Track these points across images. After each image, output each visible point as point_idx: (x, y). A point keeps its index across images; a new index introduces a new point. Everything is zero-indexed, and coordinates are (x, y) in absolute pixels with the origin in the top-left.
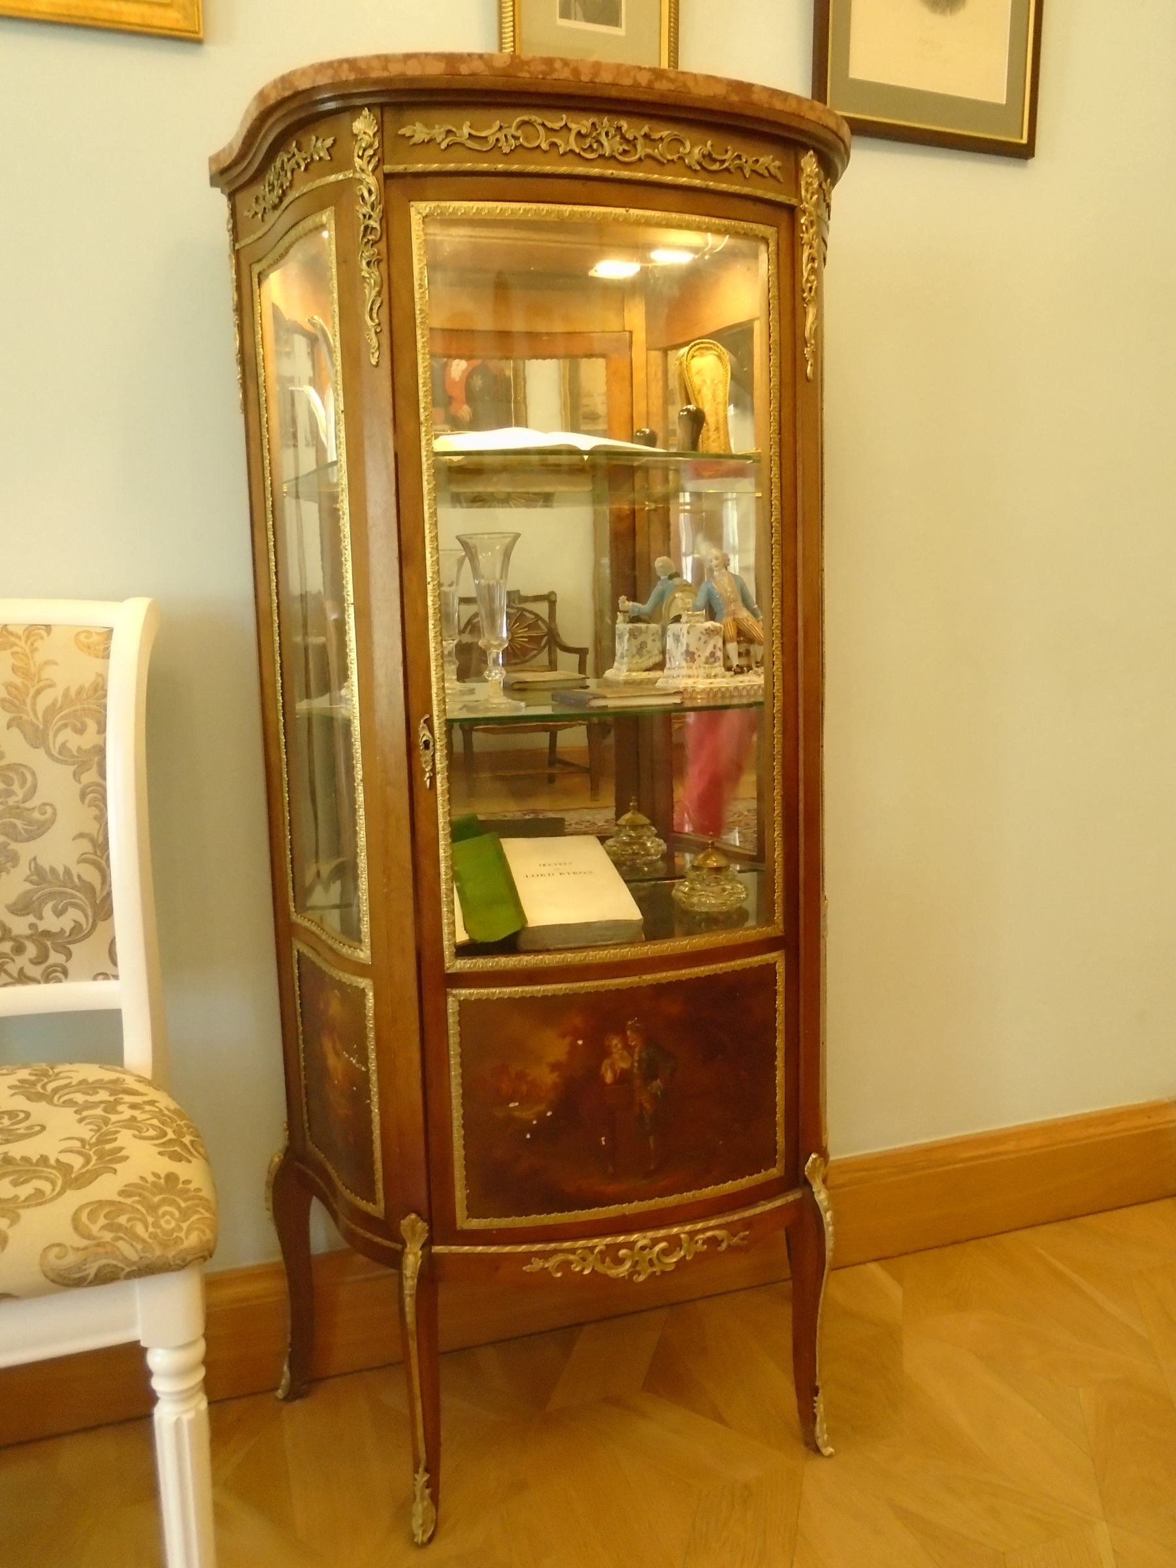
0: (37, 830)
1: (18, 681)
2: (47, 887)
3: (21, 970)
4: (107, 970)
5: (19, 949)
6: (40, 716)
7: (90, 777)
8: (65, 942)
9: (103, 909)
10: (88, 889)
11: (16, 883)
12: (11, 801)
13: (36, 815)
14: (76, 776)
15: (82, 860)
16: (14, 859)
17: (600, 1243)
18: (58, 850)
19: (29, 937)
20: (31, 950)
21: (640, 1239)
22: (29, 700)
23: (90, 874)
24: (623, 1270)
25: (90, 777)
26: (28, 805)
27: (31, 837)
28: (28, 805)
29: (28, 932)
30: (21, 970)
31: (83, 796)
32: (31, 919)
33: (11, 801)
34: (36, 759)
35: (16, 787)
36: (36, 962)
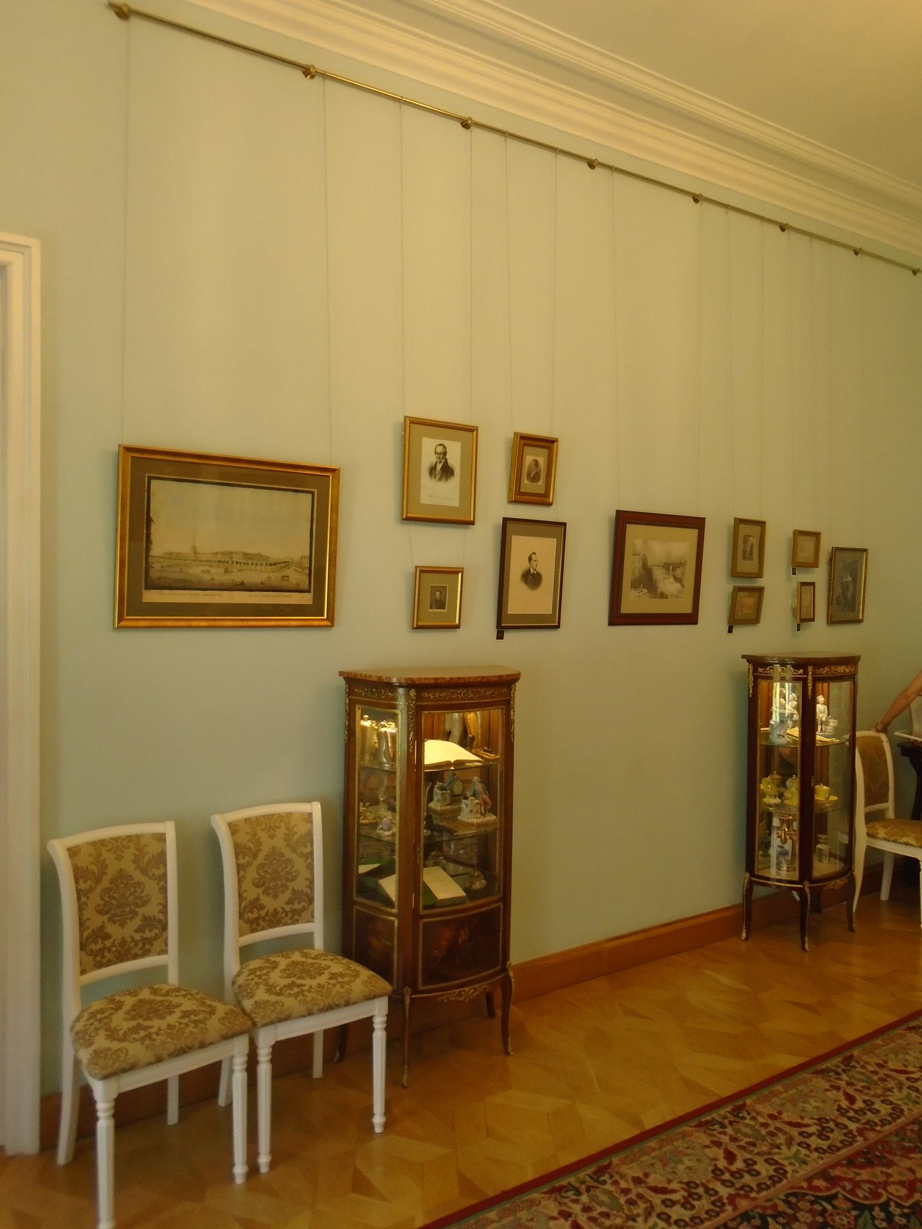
1: (137, 853)
2: (148, 922)
4: (164, 952)
14: (158, 884)
15: (159, 912)
17: (457, 991)
21: (467, 989)
24: (462, 999)
25: (162, 883)
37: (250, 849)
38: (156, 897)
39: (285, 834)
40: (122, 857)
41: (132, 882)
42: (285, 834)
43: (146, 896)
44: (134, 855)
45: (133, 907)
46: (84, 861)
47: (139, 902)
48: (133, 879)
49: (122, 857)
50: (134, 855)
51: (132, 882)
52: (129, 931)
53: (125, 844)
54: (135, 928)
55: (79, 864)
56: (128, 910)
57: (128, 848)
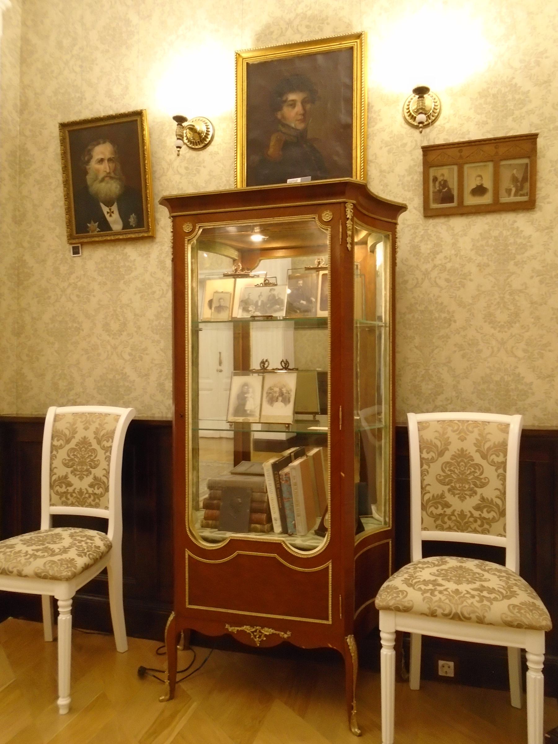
0: (483, 485)
3: (475, 528)
6: (486, 449)
12: (476, 475)
13: (483, 480)
14: (496, 470)
16: (476, 493)
20: (479, 522)
22: (482, 444)
25: (501, 471)
26: (481, 477)
27: (482, 487)
29: (478, 516)
30: (475, 528)
33: (476, 475)
34: (484, 463)
35: (477, 471)
36: (480, 526)
37: (65, 435)
39: (97, 428)
40: (466, 439)
41: (90, 448)
42: (97, 428)
44: (477, 439)
45: (89, 467)
46: (429, 435)
49: (466, 439)
50: (477, 439)
51: (90, 448)
52: (468, 505)
53: (470, 429)
54: (474, 505)
55: (425, 437)
56: (467, 486)
57: (472, 432)
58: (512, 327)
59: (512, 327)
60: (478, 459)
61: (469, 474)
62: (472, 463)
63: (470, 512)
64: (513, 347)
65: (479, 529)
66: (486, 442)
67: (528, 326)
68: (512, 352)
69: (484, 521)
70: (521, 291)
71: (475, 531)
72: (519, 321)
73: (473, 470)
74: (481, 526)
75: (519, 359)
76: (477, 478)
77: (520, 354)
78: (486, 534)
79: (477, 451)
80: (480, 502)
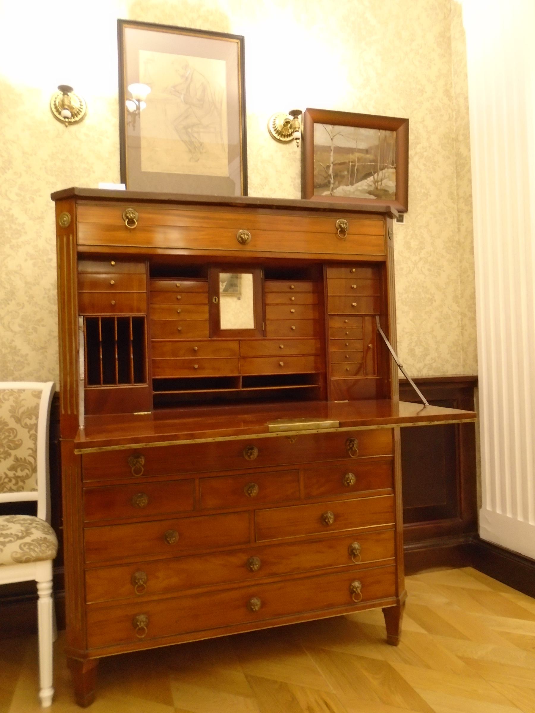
3: (10, 488)
5: (10, 481)
7: (33, 432)
8: (23, 479)
9: (34, 470)
10: (30, 463)
11: (10, 462)
12: (10, 438)
13: (17, 442)
14: (29, 432)
15: (30, 455)
16: (10, 455)
18: (23, 453)
19: (14, 478)
20: (14, 481)
23: (31, 460)
25: (33, 432)
26: (15, 439)
28: (15, 439)
30: (10, 488)
31: (30, 437)
32: (14, 472)
33: (10, 438)
34: (17, 427)
35: (11, 434)
38: (28, 443)
43: (18, 441)
47: (12, 445)
48: (8, 425)
58: (9, 304)
59: (9, 304)
60: (12, 424)
61: (4, 439)
62: (6, 428)
63: (5, 474)
64: (9, 323)
65: (14, 488)
66: (20, 408)
67: (23, 303)
68: (9, 327)
69: (19, 479)
70: (16, 272)
71: (11, 490)
72: (15, 299)
73: (7, 434)
74: (17, 483)
75: (15, 333)
76: (12, 441)
77: (16, 328)
78: (21, 491)
79: (11, 417)
80: (14, 463)
